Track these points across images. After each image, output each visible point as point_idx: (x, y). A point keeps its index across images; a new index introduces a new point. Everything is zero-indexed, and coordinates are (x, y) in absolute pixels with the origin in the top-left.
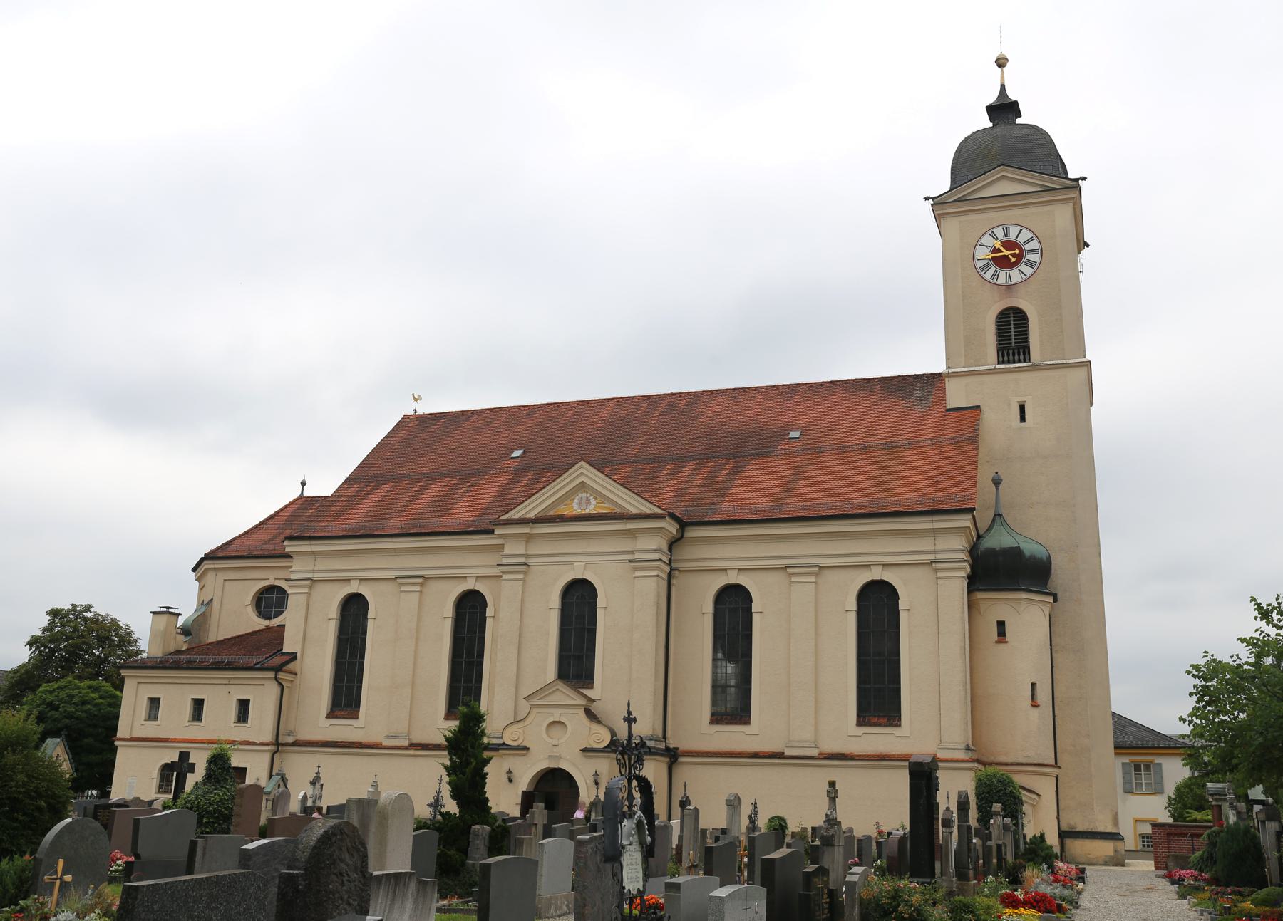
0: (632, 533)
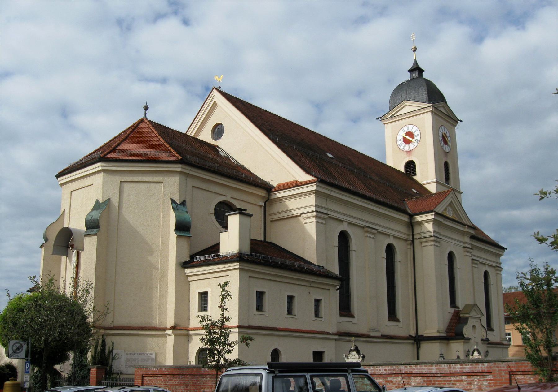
0: (463, 233)
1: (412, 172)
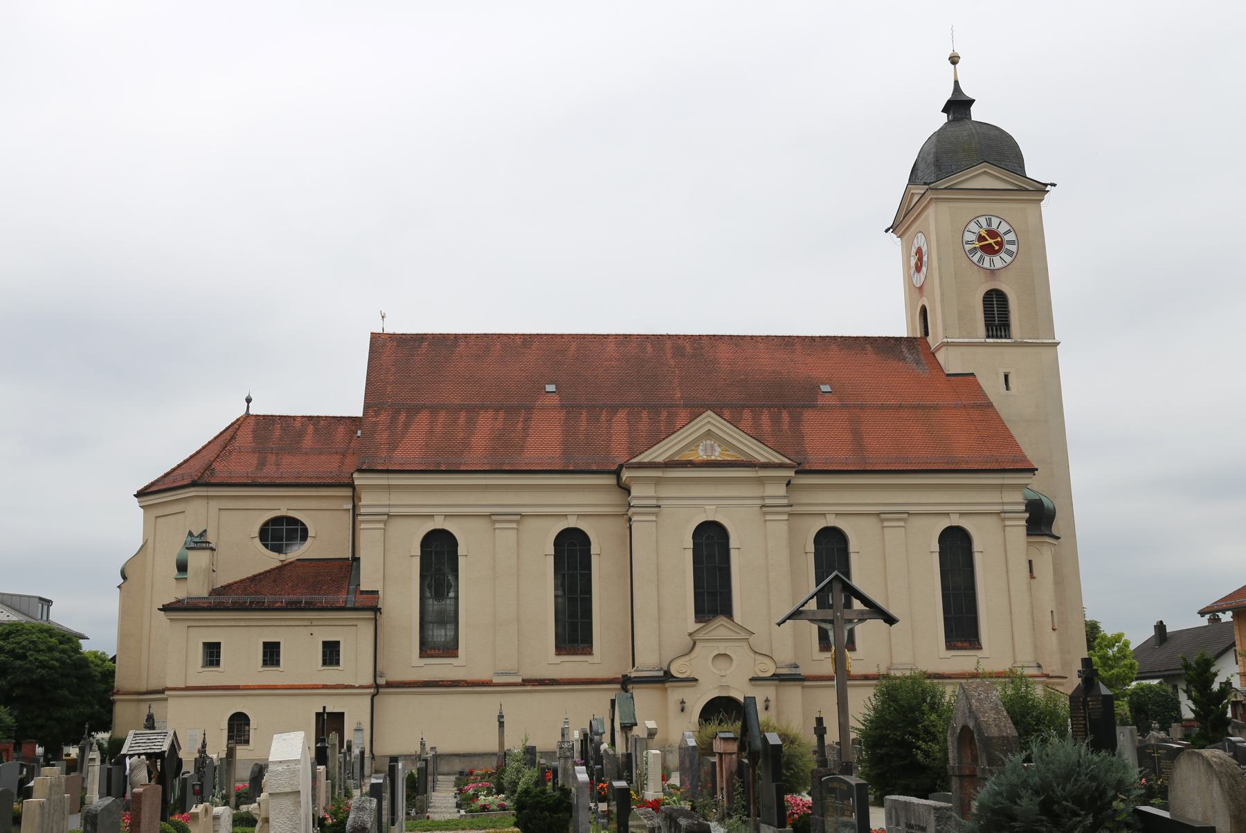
0: (761, 481)
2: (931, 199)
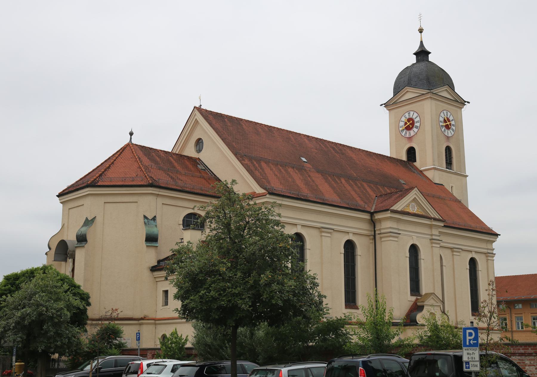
0: (431, 227)
1: (413, 159)
2: (430, 97)
